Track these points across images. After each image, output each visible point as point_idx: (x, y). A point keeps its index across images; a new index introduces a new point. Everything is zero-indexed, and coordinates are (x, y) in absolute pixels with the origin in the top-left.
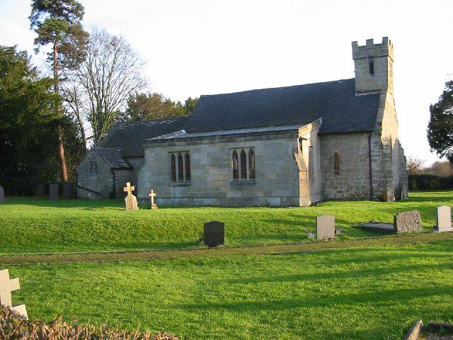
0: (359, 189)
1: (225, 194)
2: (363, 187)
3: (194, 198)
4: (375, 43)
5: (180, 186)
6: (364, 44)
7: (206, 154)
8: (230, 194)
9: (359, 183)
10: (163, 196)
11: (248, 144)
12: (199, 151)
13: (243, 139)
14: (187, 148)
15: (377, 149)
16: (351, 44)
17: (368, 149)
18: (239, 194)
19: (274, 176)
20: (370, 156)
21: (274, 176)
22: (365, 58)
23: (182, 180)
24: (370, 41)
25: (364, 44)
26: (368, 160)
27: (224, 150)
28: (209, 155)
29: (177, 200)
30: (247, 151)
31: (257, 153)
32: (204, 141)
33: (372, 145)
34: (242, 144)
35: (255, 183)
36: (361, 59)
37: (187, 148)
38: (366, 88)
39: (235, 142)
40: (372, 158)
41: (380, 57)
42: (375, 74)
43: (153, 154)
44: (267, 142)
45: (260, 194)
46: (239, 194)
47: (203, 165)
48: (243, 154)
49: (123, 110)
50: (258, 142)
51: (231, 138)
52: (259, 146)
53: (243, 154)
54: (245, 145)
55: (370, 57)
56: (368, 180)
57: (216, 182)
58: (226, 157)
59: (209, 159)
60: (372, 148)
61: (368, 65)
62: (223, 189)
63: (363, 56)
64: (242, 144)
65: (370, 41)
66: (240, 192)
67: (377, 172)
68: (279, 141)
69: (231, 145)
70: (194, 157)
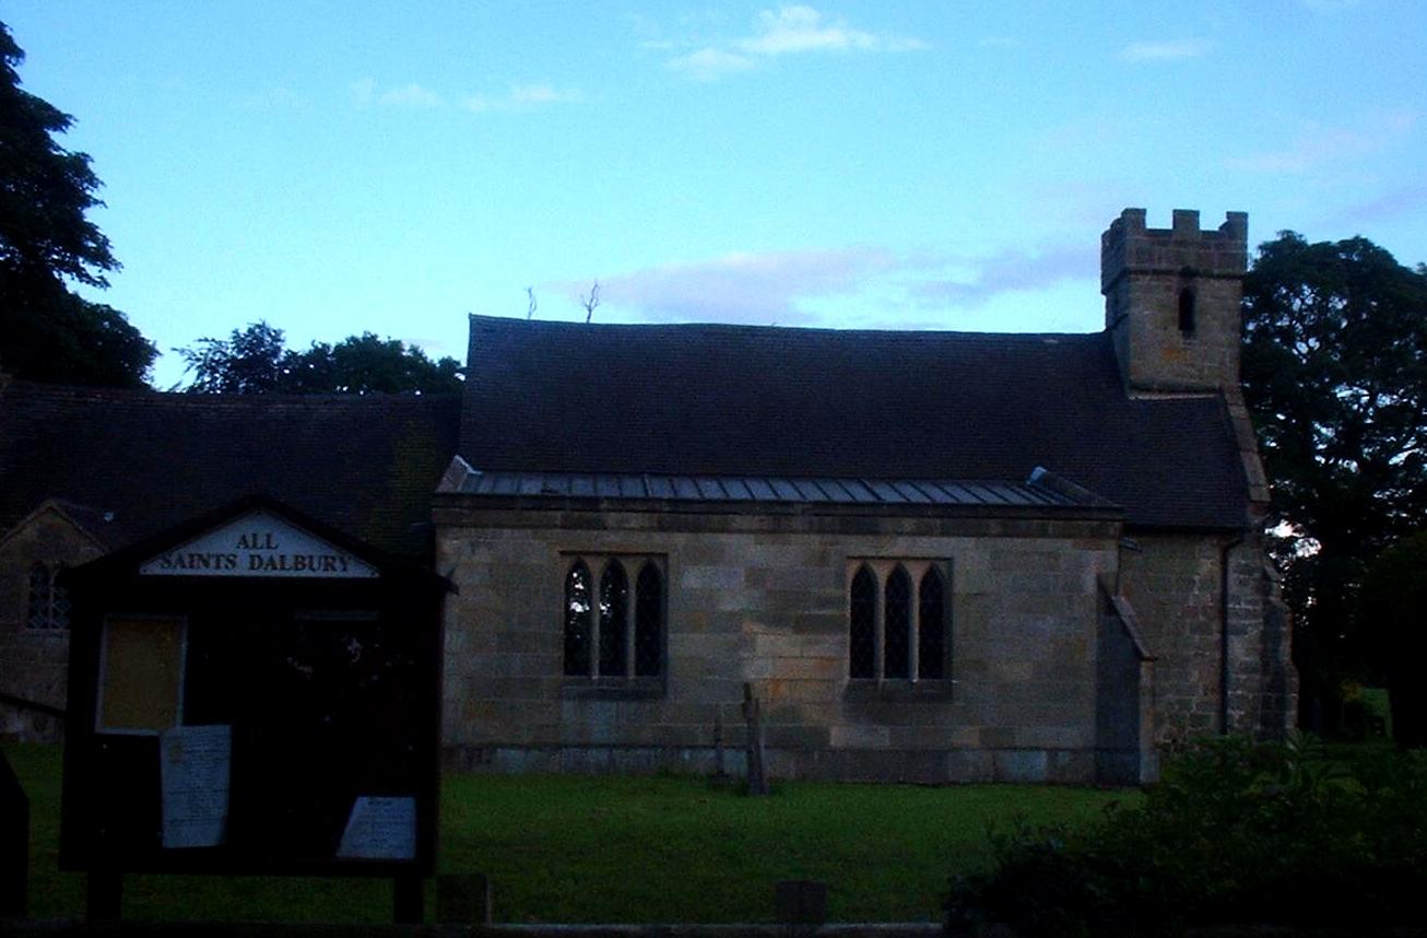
0: (1182, 729)
1: (821, 734)
2: (1198, 720)
3: (679, 748)
4: (1149, 226)
5: (604, 695)
6: (1167, 223)
7: (742, 571)
8: (841, 735)
9: (1184, 705)
10: (527, 739)
11: (929, 546)
12: (712, 557)
13: (908, 524)
14: (658, 541)
15: (1248, 593)
16: (1140, 207)
17: (1217, 591)
18: (881, 738)
19: (1020, 672)
20: (1223, 613)
21: (1020, 672)
22: (1168, 272)
23: (622, 671)
24: (1186, 218)
25: (1167, 223)
26: (1216, 626)
27: (823, 559)
28: (756, 577)
29: (598, 756)
30: (916, 574)
31: (960, 586)
32: (739, 521)
33: (1232, 577)
34: (900, 546)
35: (947, 695)
36: (1156, 272)
37: (658, 541)
38: (1166, 376)
39: (875, 533)
40: (1232, 621)
41: (1218, 277)
42: (1199, 331)
43: (483, 556)
44: (1003, 543)
45: (966, 736)
46: (881, 738)
47: (732, 614)
48: (899, 580)
49: (1132, 378)
50: (969, 542)
51: (860, 519)
52: (971, 560)
53: (899, 580)
54: (914, 548)
55: (1188, 274)
56: (1214, 698)
57: (783, 688)
58: (832, 591)
59: (756, 593)
60: (1233, 589)
61: (1174, 297)
62: (813, 716)
63: (1164, 266)
64: (900, 546)
65: (1186, 218)
66: (885, 730)
67: (1247, 669)
68: (1046, 544)
69: (859, 545)
70: (689, 580)
